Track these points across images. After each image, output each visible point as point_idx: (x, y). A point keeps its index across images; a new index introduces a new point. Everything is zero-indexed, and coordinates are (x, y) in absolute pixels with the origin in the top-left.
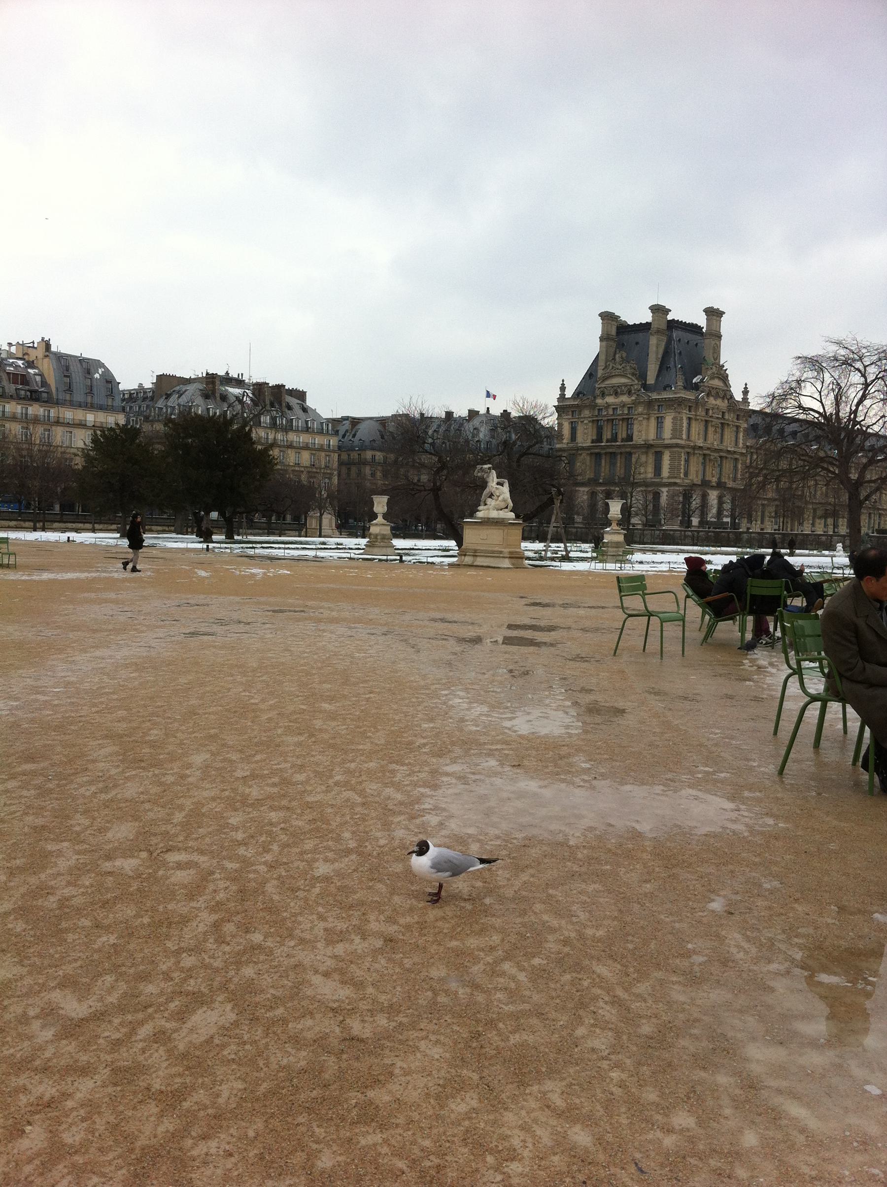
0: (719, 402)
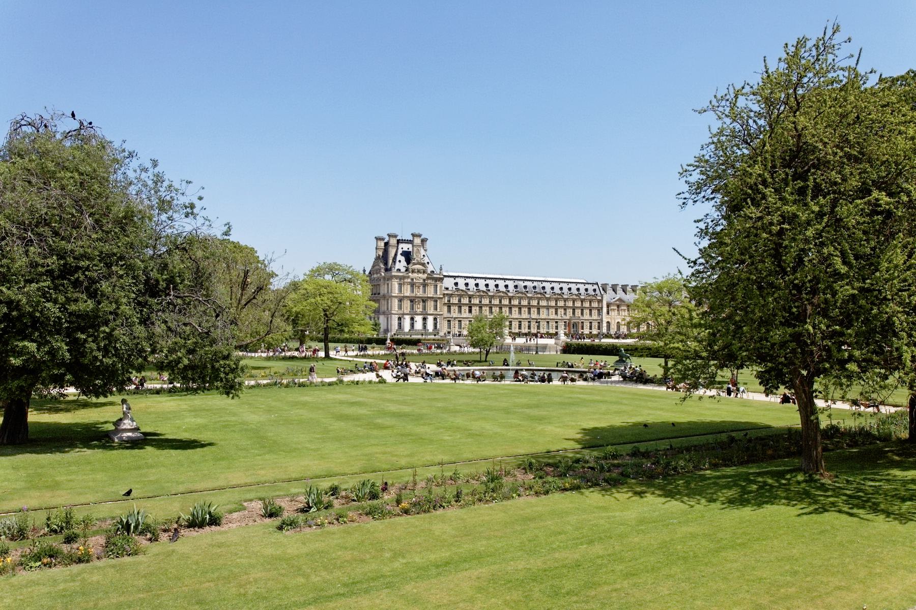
0: (420, 275)
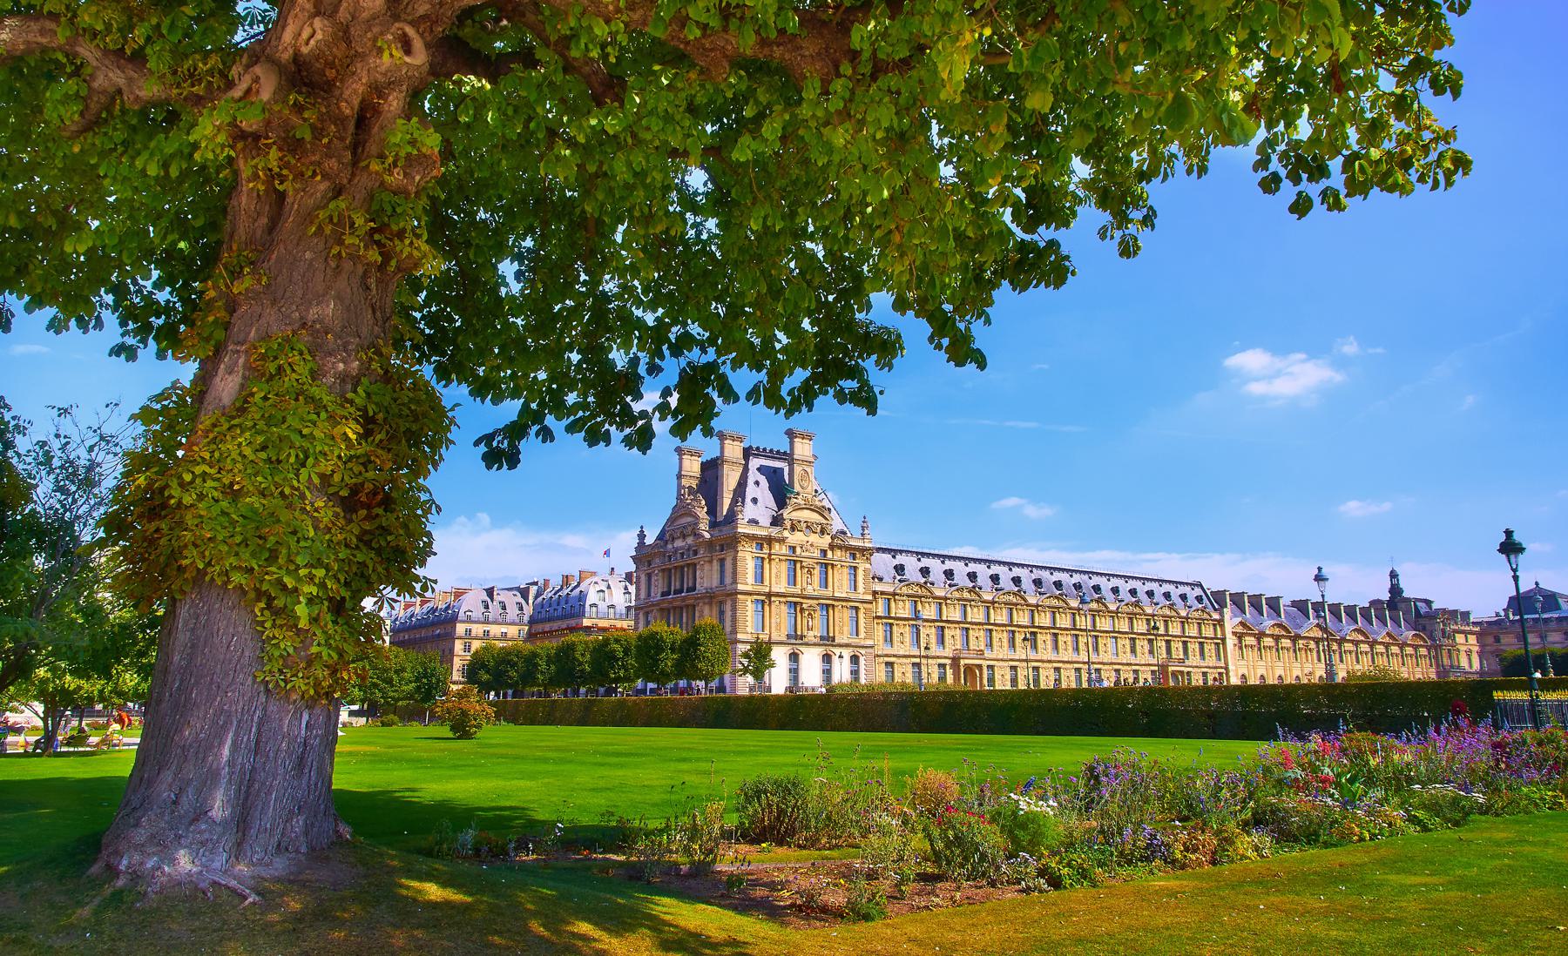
0: (814, 538)
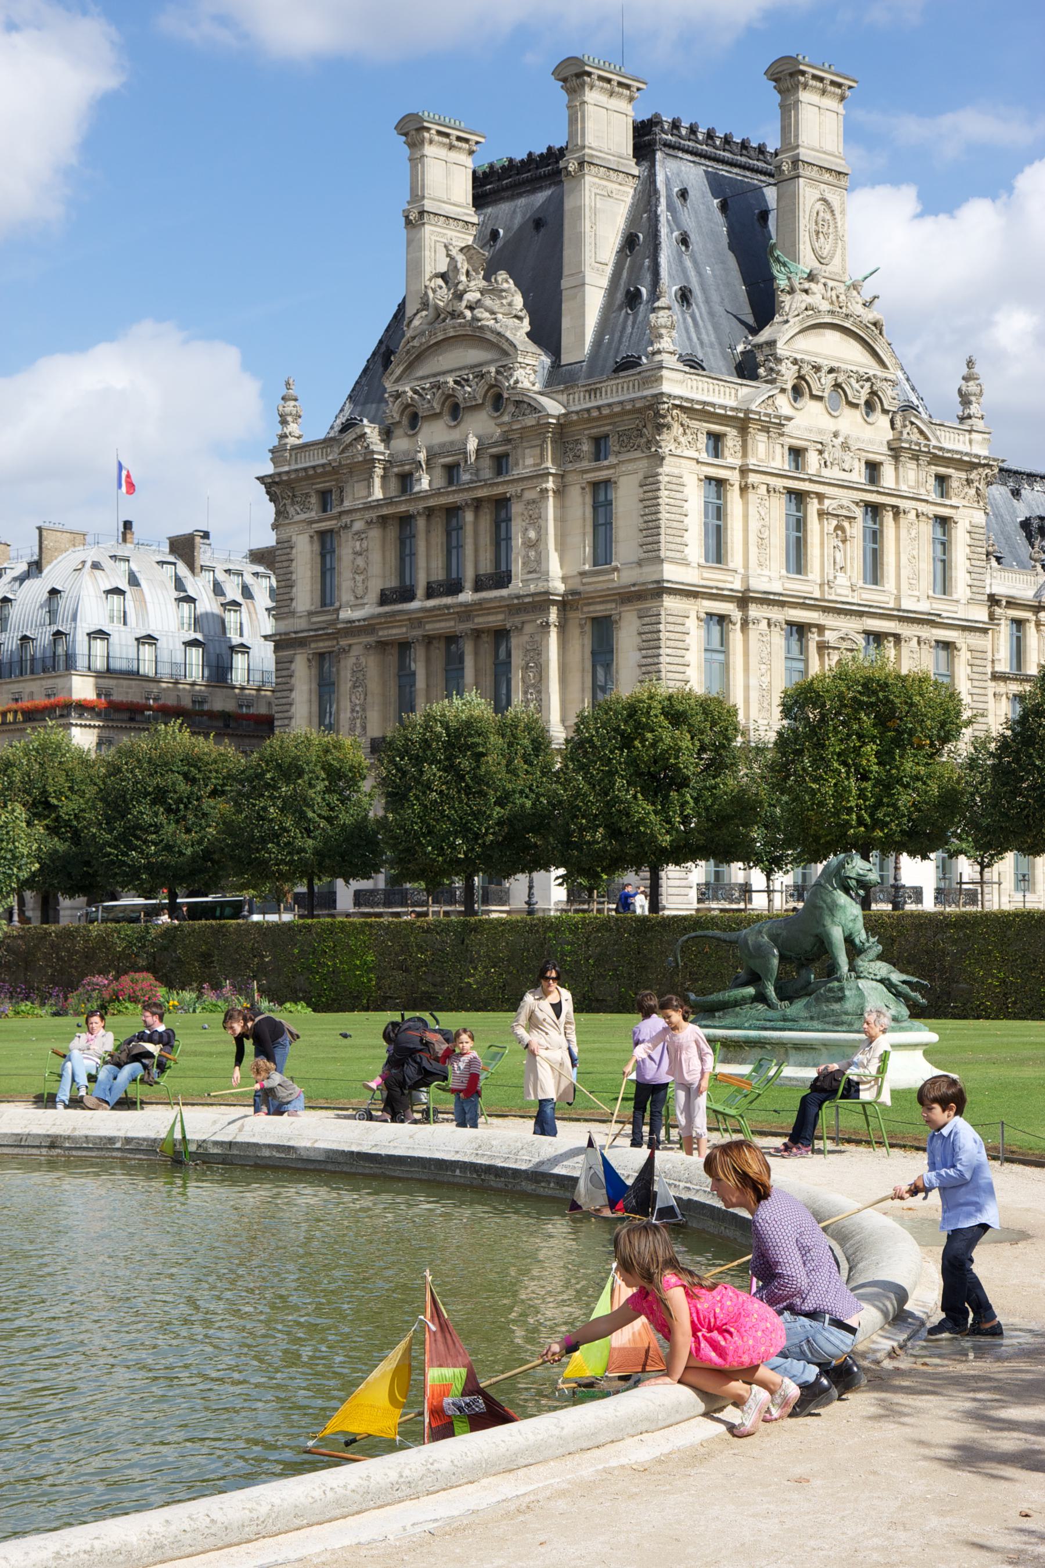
0: (850, 422)
